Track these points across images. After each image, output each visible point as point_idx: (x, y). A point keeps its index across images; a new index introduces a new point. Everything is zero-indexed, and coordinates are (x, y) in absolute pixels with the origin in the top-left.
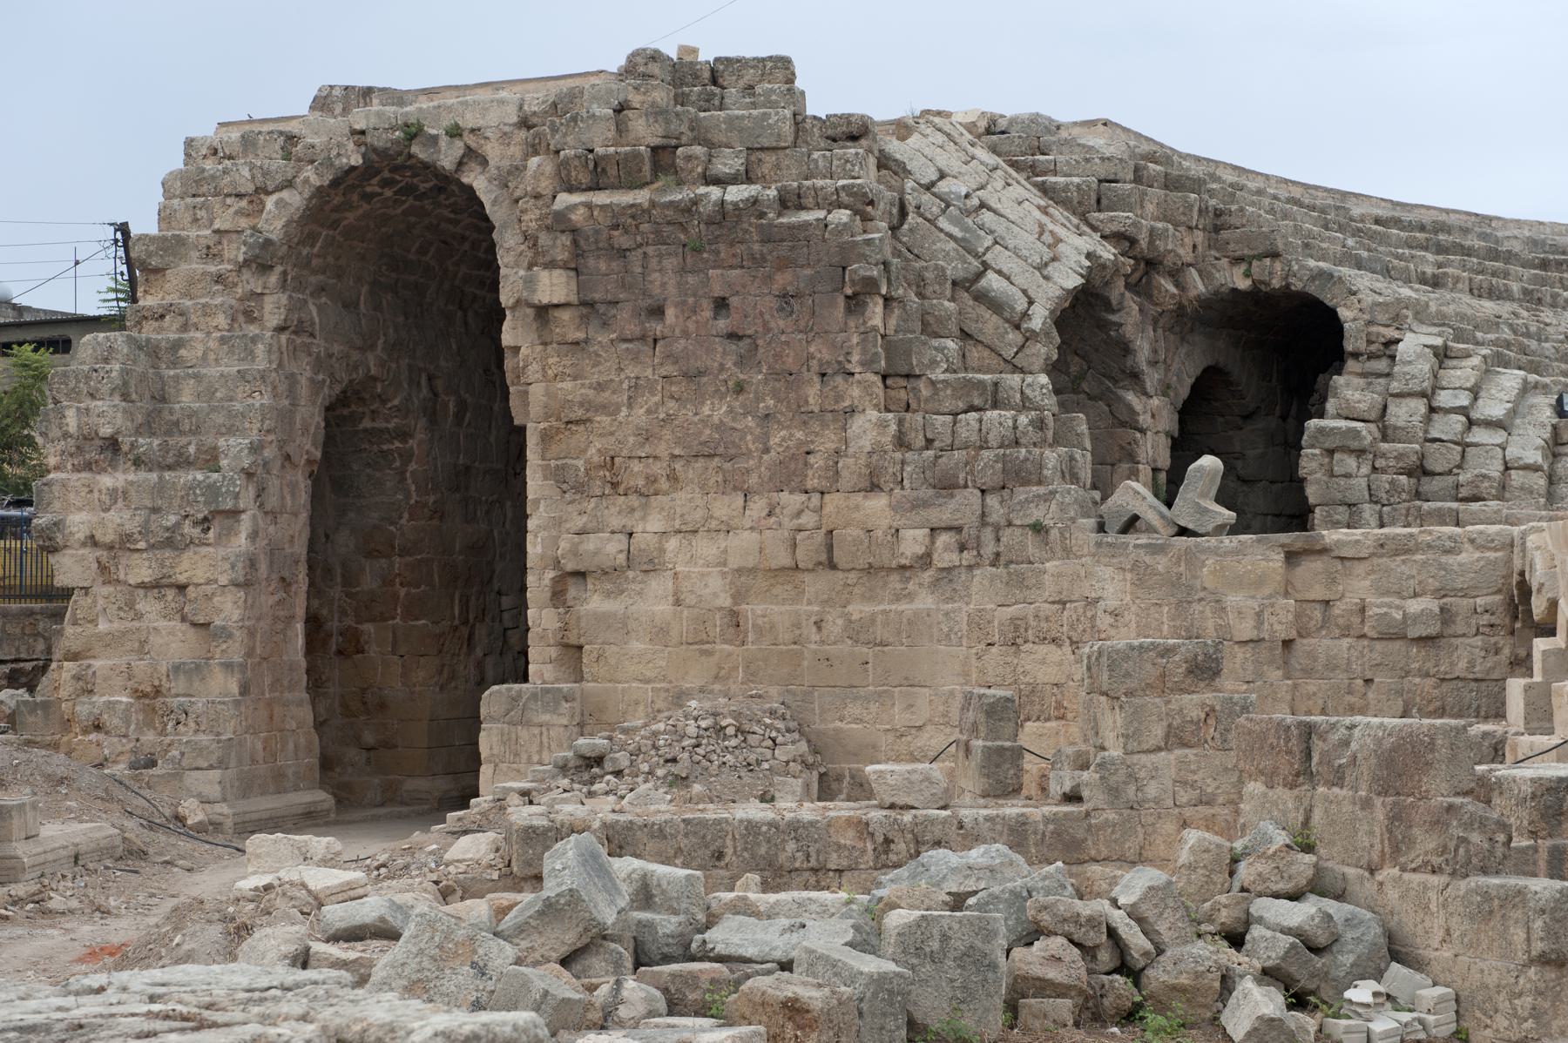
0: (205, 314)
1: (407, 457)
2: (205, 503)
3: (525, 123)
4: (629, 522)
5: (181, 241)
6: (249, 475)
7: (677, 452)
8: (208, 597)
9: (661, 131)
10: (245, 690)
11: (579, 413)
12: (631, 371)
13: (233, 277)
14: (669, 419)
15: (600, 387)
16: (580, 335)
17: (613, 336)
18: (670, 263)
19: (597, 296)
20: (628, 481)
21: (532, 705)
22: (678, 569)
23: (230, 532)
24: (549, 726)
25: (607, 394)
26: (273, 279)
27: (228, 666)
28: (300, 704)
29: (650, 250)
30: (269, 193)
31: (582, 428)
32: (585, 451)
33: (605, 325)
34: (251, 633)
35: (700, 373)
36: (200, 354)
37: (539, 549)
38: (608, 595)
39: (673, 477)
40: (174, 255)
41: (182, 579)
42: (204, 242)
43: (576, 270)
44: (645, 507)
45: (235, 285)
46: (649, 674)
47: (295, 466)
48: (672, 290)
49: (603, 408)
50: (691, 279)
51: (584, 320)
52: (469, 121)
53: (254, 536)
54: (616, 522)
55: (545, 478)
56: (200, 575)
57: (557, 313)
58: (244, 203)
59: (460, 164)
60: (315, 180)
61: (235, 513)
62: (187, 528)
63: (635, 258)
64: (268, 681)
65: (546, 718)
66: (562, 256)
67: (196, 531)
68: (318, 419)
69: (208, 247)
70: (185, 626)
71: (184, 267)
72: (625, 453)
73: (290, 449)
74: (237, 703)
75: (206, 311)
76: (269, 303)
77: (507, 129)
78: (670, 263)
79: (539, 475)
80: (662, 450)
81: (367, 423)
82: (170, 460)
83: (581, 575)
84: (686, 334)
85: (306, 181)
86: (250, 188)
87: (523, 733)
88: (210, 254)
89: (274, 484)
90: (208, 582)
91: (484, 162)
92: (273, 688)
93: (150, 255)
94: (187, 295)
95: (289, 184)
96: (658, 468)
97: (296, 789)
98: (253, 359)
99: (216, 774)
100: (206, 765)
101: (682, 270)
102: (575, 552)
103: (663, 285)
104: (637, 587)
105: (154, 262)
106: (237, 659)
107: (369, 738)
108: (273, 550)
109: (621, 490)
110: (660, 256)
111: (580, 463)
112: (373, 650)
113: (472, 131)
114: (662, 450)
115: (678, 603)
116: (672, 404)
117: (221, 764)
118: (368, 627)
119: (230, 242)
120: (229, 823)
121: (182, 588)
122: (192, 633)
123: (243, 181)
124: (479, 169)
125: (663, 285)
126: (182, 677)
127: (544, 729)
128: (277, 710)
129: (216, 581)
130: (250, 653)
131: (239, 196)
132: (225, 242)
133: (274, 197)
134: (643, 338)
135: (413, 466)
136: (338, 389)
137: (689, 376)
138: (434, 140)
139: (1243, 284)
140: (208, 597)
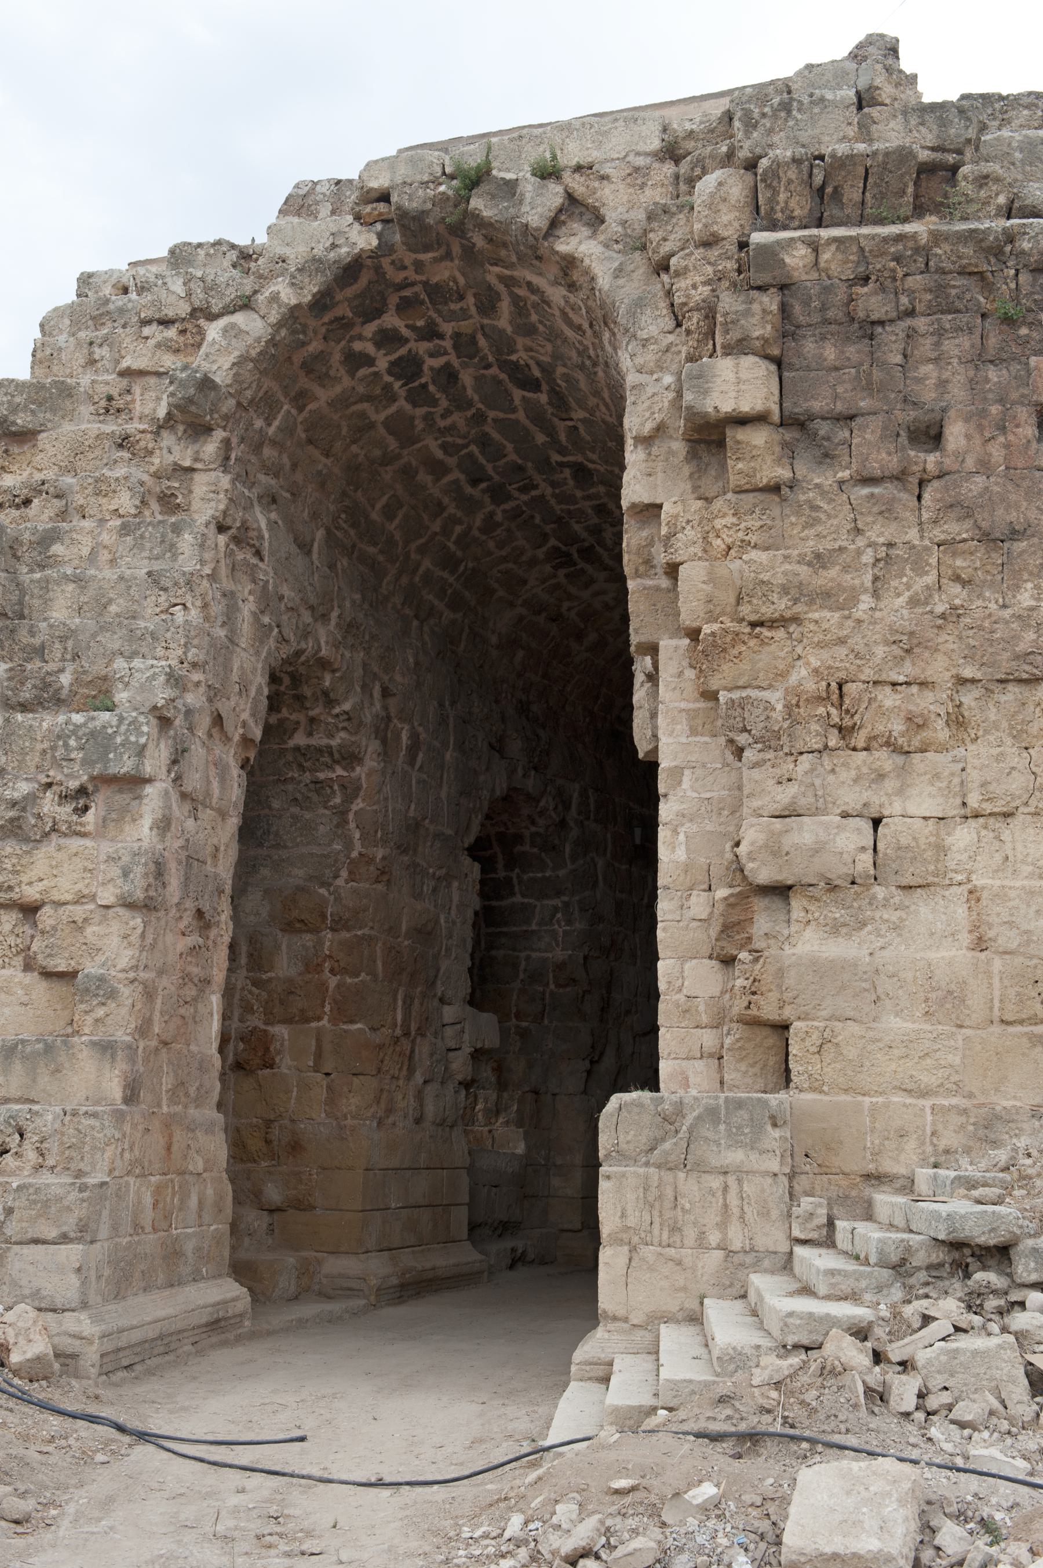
0: (98, 493)
1: (351, 790)
2: (85, 762)
3: (671, 152)
4: (878, 799)
5: (66, 391)
6: (165, 722)
7: (968, 673)
8: (77, 926)
9: (930, 140)
10: (131, 1095)
11: (781, 605)
12: (879, 532)
13: (147, 441)
14: (954, 614)
15: (819, 560)
16: (783, 473)
17: (845, 474)
18: (957, 346)
19: (817, 406)
20: (871, 724)
21: (706, 1130)
22: (978, 881)
23: (123, 816)
24: (741, 1173)
25: (833, 572)
26: (211, 447)
27: (106, 1048)
28: (209, 1131)
29: (921, 323)
30: (212, 317)
31: (780, 634)
32: (783, 675)
33: (826, 457)
34: (149, 994)
35: (1014, 534)
36: (85, 551)
37: (681, 855)
38: (835, 929)
39: (958, 721)
40: (54, 410)
41: (31, 893)
42: (102, 390)
43: (778, 362)
44: (903, 771)
45: (150, 453)
46: (927, 1079)
47: (227, 739)
48: (958, 392)
49: (826, 597)
50: (993, 374)
51: (789, 452)
52: (572, 154)
53: (164, 825)
54: (851, 798)
55: (693, 732)
56: (65, 887)
57: (742, 434)
58: (172, 333)
59: (554, 223)
60: (289, 296)
61: (136, 782)
62: (49, 804)
63: (892, 338)
64: (167, 1082)
65: (735, 1157)
66: (760, 329)
67: (65, 811)
68: (259, 681)
69: (110, 398)
70: (31, 978)
71: (67, 427)
72: (868, 674)
73: (224, 707)
74: (119, 1117)
75: (102, 488)
76: (201, 484)
77: (640, 161)
78: (957, 346)
79: (682, 727)
80: (939, 669)
81: (300, 739)
82: (26, 694)
83: (781, 891)
84: (985, 467)
85: (275, 298)
86: (183, 309)
87: (689, 1186)
88: (110, 408)
89: (198, 752)
90: (80, 899)
91: (596, 220)
92: (173, 1092)
93: (15, 409)
94: (70, 469)
95: (246, 304)
96: (925, 702)
97: (196, 1277)
98: (175, 557)
99: (72, 1253)
100: (52, 1233)
101: (980, 359)
102: (774, 850)
103: (942, 384)
104: (894, 916)
105: (21, 420)
106: (122, 1036)
107: (273, 1193)
108: (191, 860)
109: (860, 740)
110: (940, 333)
111: (776, 698)
112: (286, 1064)
113: (578, 168)
114: (939, 669)
115: (980, 944)
116: (957, 593)
117: (84, 1233)
118: (281, 1031)
119: (145, 389)
120: (91, 1355)
121: (30, 910)
122: (41, 988)
123: (172, 299)
124: (585, 231)
125: (942, 384)
126: (18, 1067)
127: (731, 1180)
128: (179, 1136)
129: (93, 898)
130: (143, 1030)
131: (165, 322)
132: (137, 390)
133: (222, 322)
134: (899, 477)
135: (358, 805)
136: (285, 651)
137: (987, 538)
138: (510, 187)
140: (77, 926)
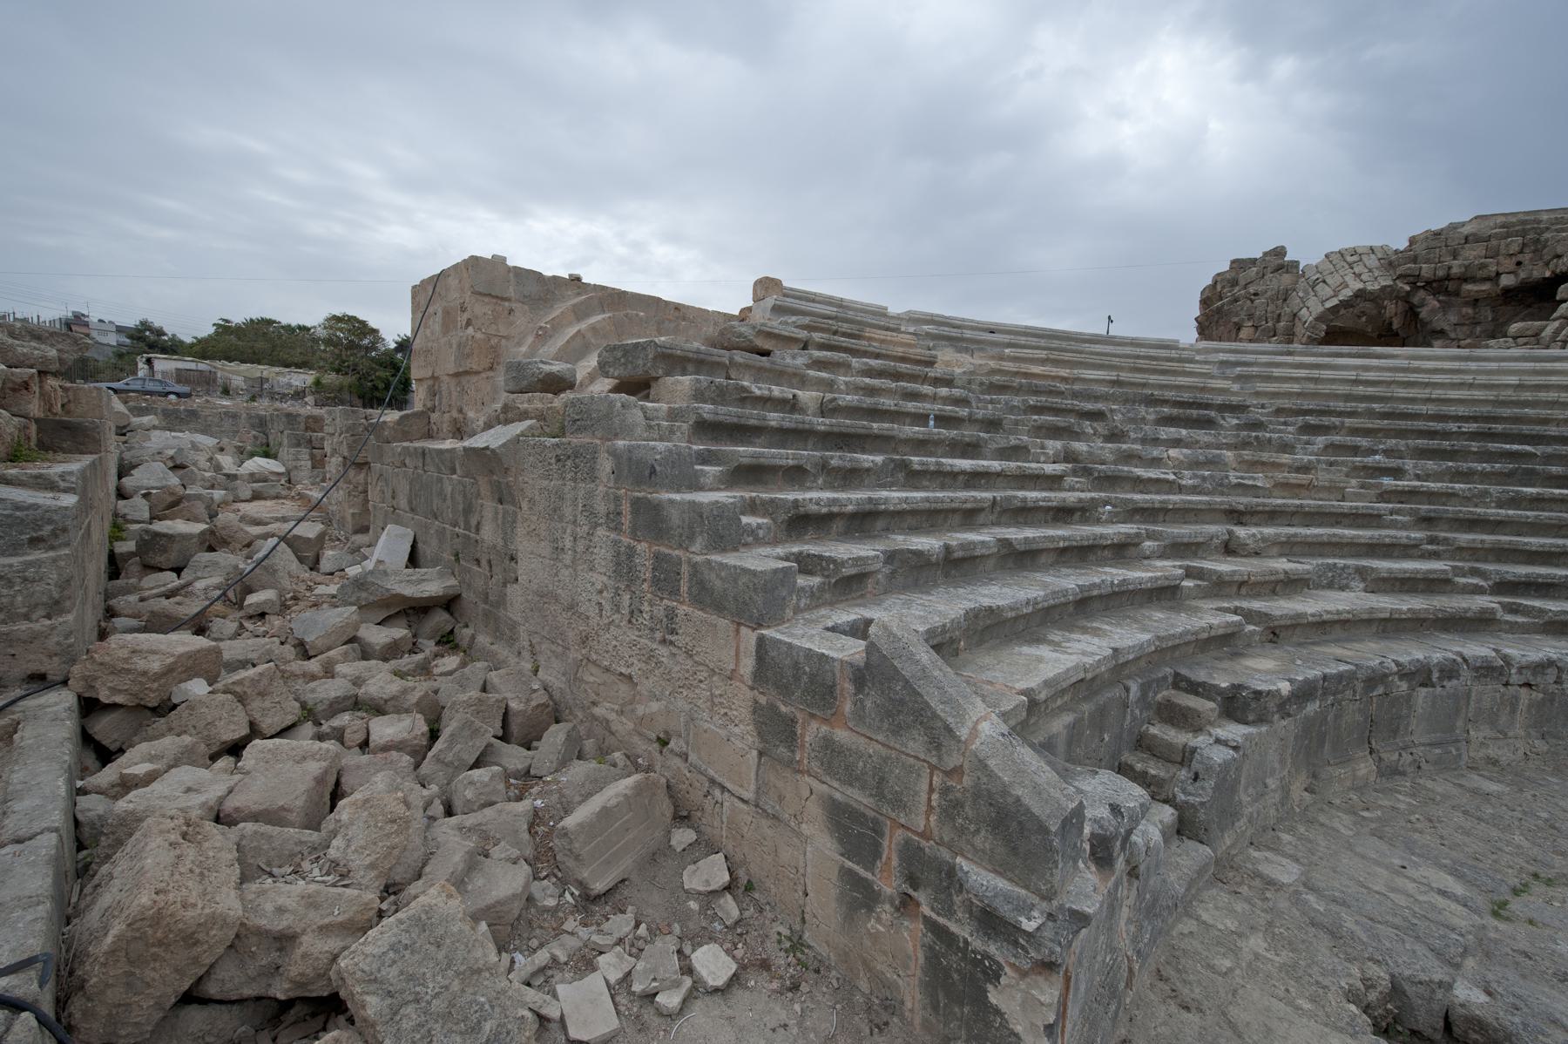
139: (1548, 274)
